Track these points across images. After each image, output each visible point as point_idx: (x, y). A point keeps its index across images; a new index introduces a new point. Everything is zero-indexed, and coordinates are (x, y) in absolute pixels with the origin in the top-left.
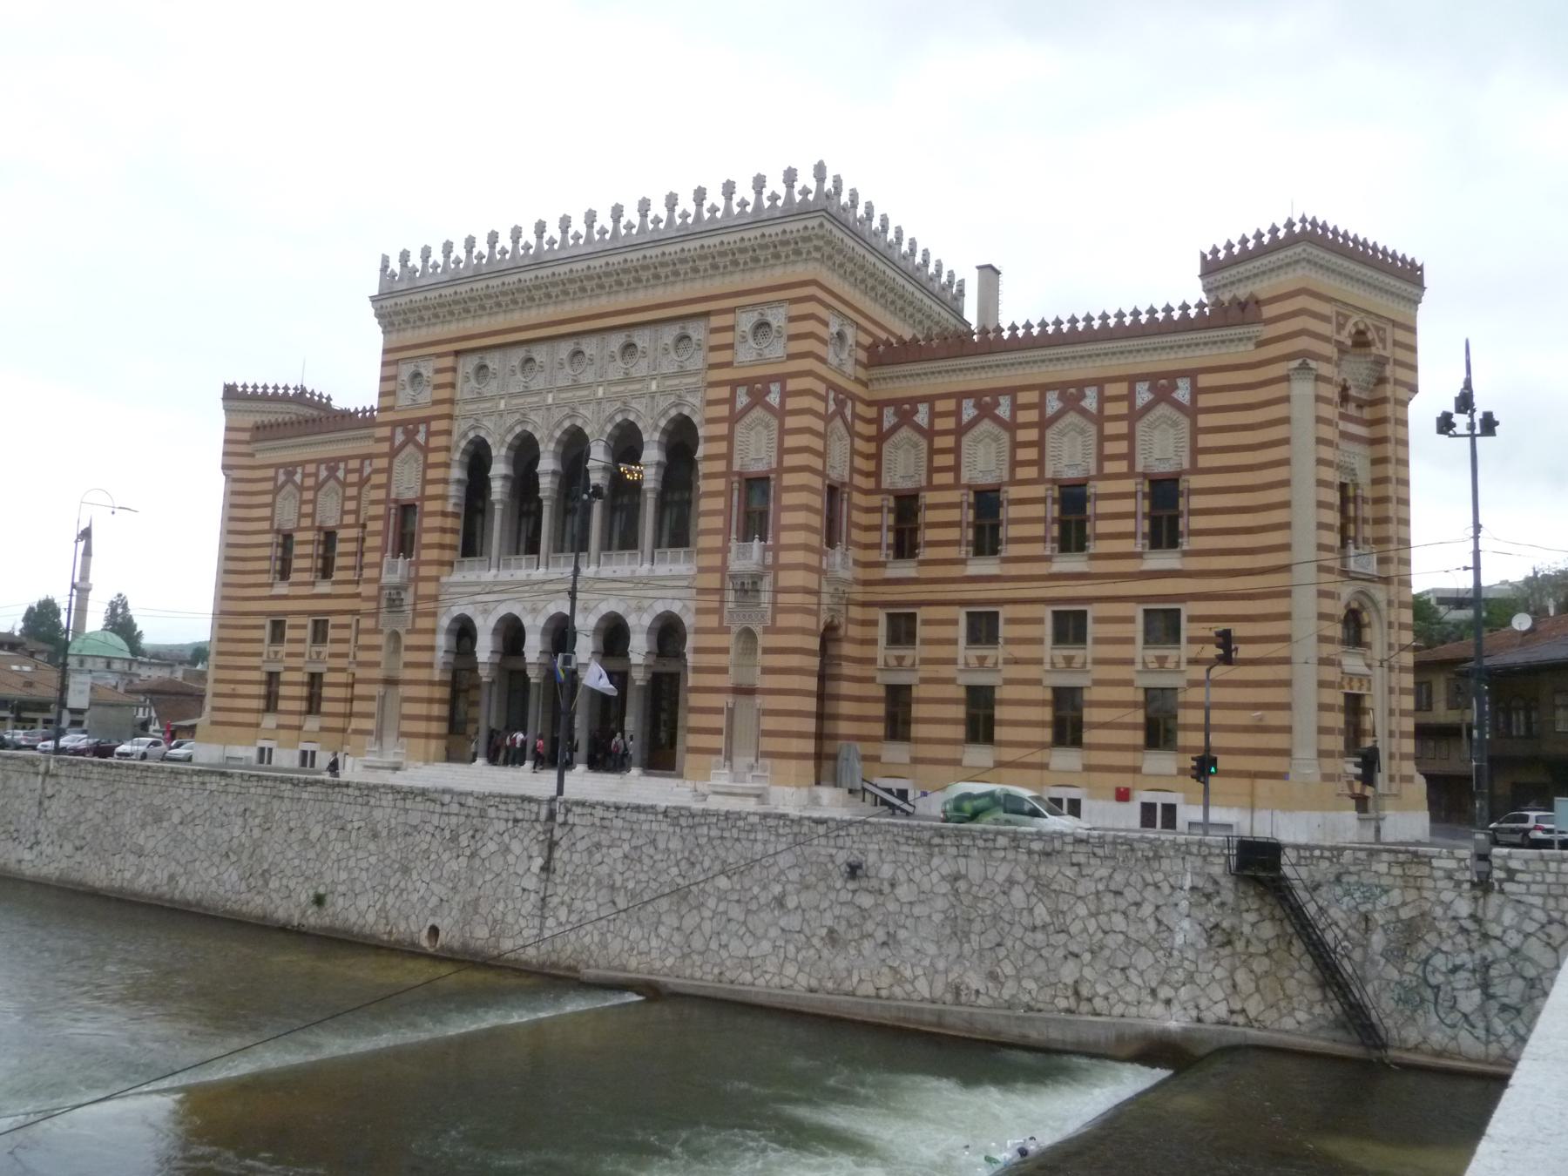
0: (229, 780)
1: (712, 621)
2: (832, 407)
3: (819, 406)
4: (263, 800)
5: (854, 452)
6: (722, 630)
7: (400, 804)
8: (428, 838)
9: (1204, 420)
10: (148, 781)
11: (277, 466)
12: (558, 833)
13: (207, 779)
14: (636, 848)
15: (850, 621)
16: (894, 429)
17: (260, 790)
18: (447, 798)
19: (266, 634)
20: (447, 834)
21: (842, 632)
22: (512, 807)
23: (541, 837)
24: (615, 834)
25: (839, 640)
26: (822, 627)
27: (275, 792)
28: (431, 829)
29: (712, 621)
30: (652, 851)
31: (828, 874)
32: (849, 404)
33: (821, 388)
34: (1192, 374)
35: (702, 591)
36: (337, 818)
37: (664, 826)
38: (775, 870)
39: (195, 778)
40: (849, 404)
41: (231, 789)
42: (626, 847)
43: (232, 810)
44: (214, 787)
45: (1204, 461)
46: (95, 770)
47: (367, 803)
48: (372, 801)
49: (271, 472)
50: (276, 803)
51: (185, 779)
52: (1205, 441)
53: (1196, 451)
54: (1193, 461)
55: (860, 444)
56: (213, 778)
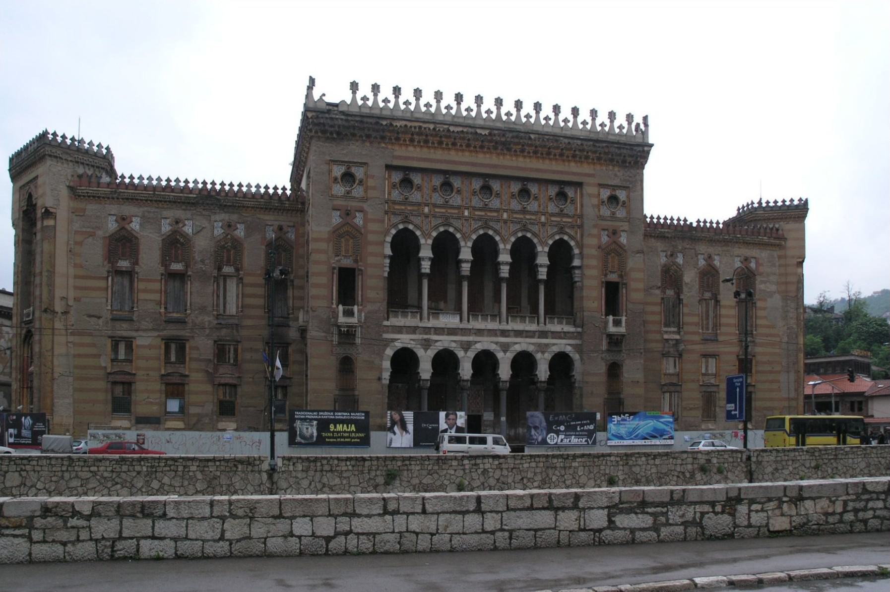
0: (502, 461)
4: (538, 470)
7: (651, 462)
8: (675, 478)
10: (413, 467)
12: (754, 467)
13: (479, 461)
14: (795, 468)
17: (533, 465)
18: (685, 456)
20: (688, 475)
22: (726, 456)
23: (745, 470)
24: (784, 463)
27: (548, 464)
28: (676, 474)
30: (803, 468)
31: (879, 468)
36: (605, 475)
37: (807, 457)
38: (858, 470)
39: (466, 462)
41: (504, 466)
42: (791, 468)
43: (510, 481)
44: (487, 466)
46: (343, 463)
47: (627, 464)
48: (631, 463)
50: (550, 472)
51: (454, 463)
56: (486, 461)
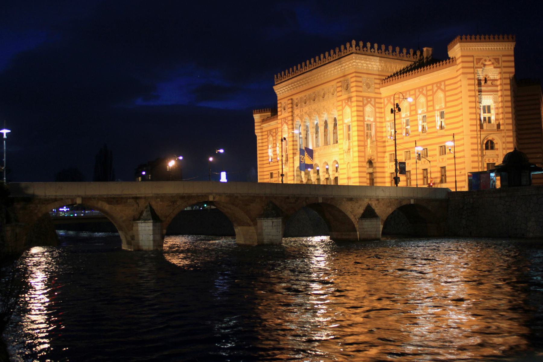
1: (342, 161)
2: (365, 102)
3: (361, 104)
5: (376, 112)
6: (344, 164)
9: (448, 94)
11: (267, 131)
15: (378, 157)
16: (387, 104)
19: (269, 176)
21: (375, 161)
25: (375, 163)
26: (367, 160)
29: (342, 161)
32: (373, 99)
33: (361, 99)
34: (444, 81)
35: (340, 154)
40: (373, 99)
45: (448, 105)
49: (266, 133)
52: (448, 99)
53: (446, 102)
54: (446, 105)
55: (377, 110)
